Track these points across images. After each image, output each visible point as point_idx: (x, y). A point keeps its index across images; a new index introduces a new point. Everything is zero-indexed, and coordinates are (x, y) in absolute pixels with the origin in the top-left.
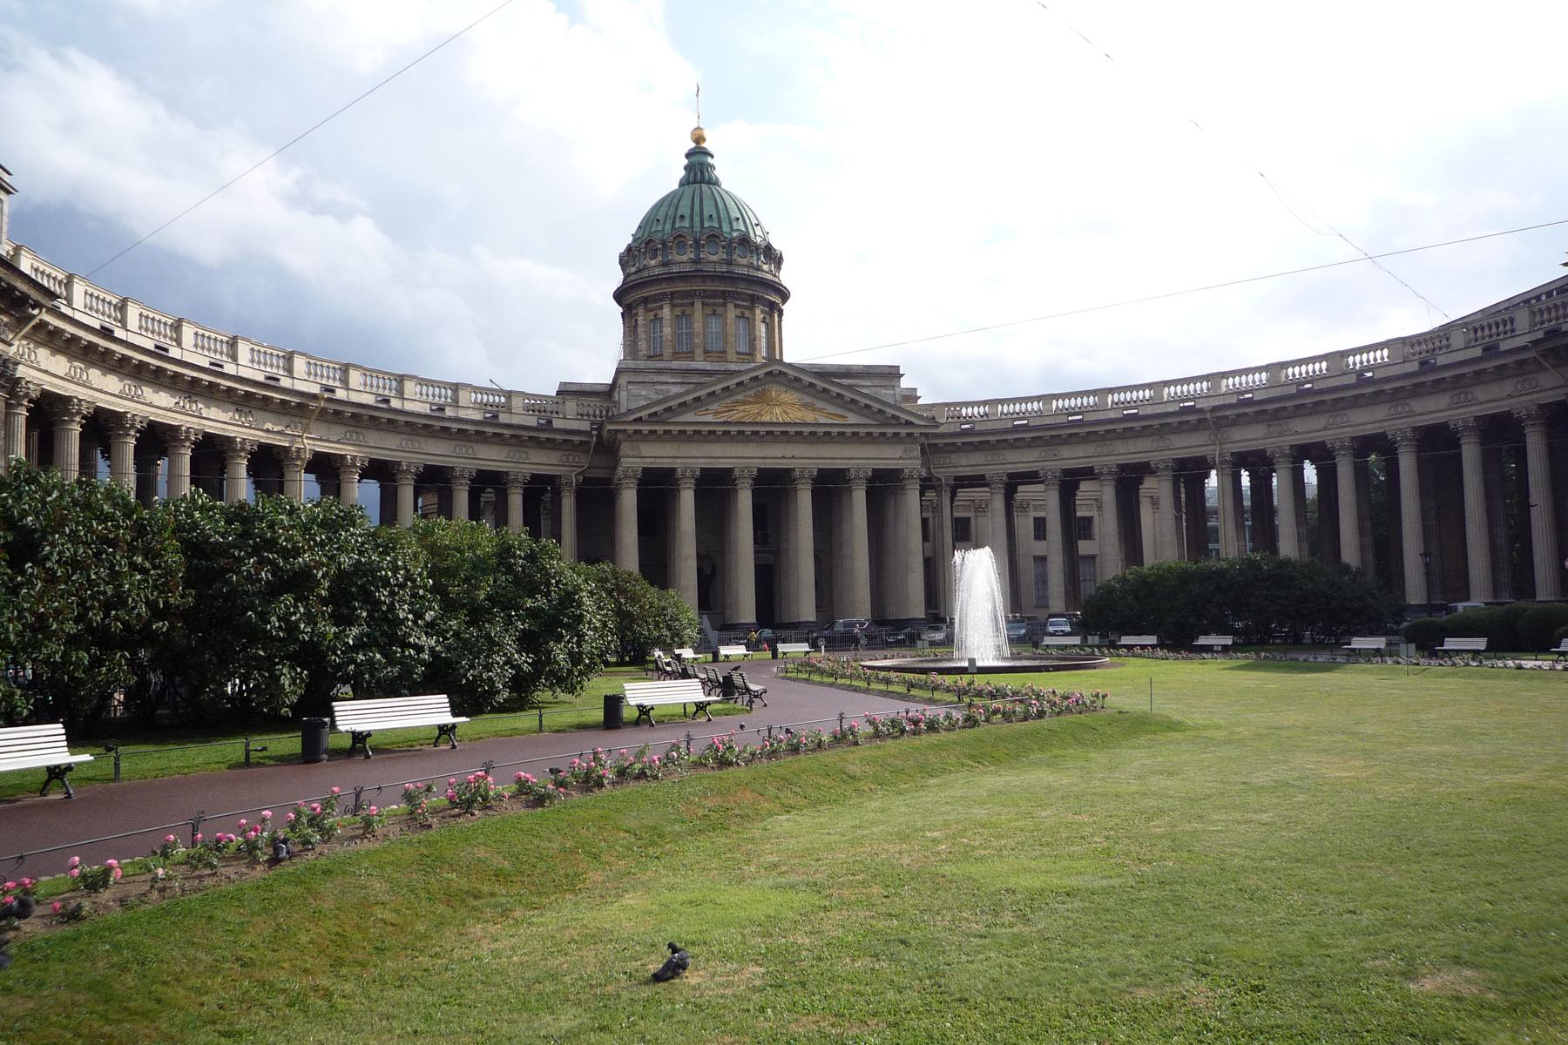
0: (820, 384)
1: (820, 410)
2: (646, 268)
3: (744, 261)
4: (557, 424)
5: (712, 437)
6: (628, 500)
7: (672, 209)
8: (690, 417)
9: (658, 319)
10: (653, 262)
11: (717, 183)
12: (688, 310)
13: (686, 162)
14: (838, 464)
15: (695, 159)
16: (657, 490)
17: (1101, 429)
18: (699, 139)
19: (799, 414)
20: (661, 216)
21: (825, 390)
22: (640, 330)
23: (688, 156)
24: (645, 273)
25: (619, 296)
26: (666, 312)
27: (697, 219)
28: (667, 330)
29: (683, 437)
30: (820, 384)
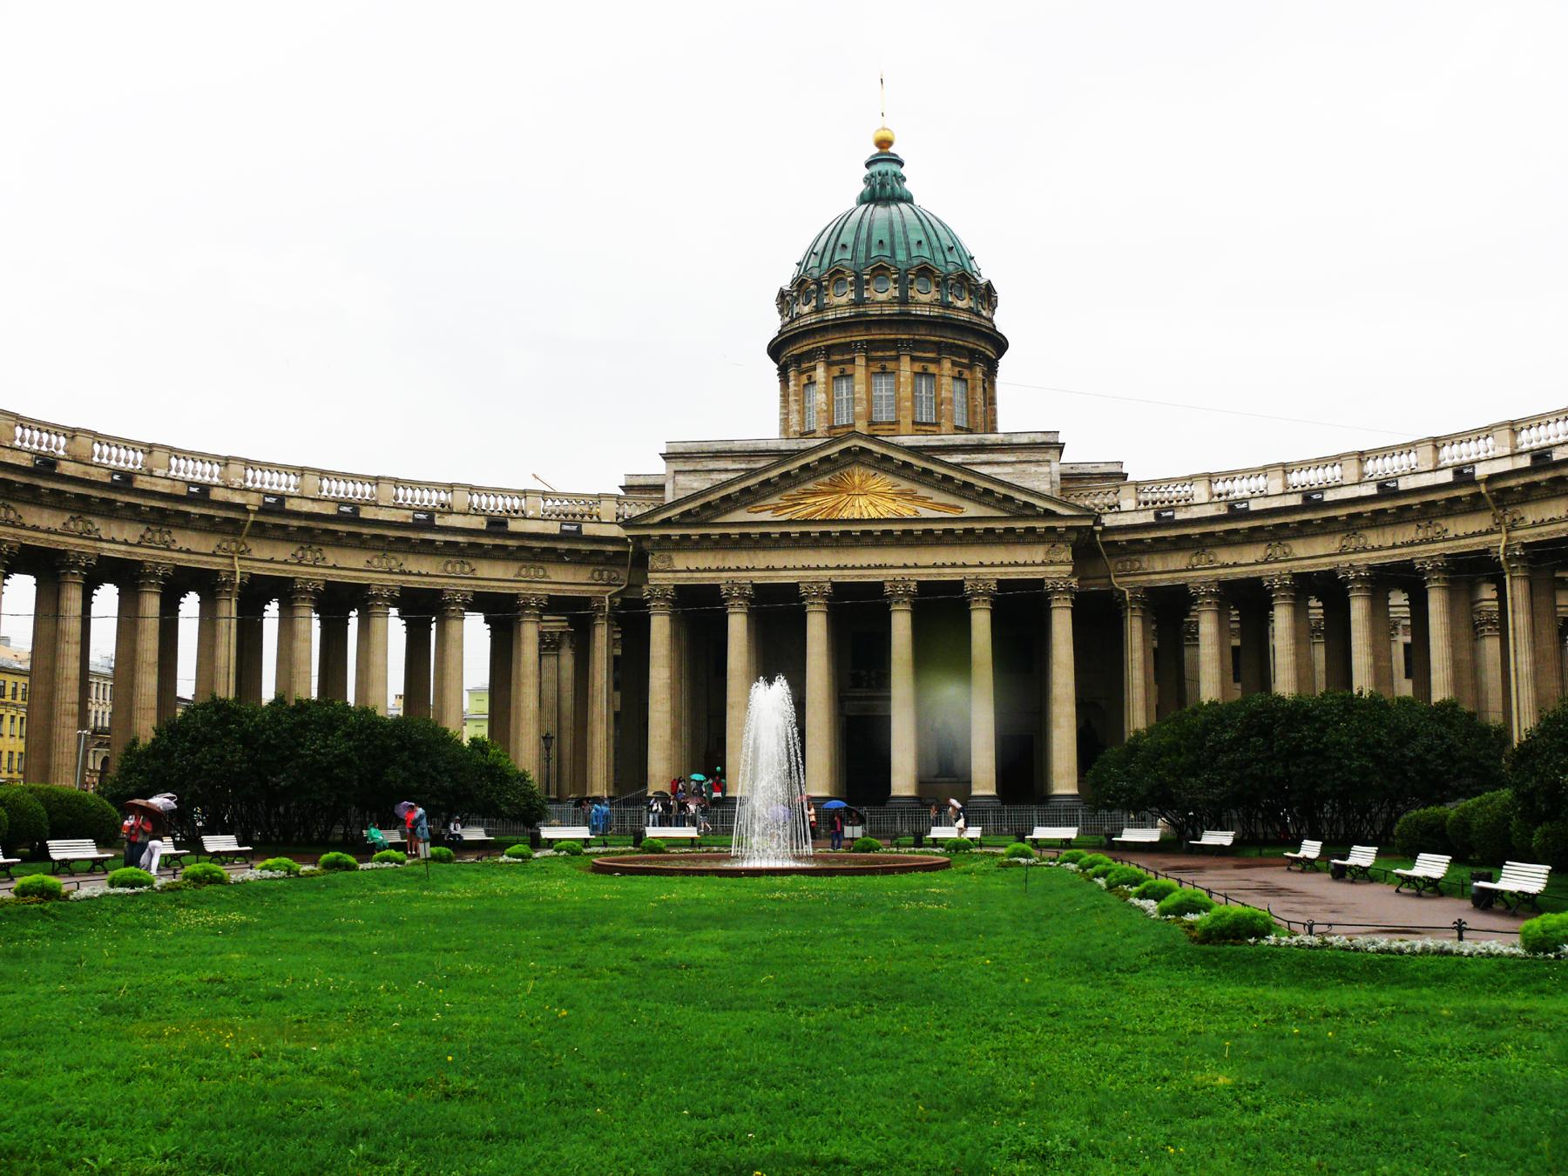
0: (919, 464)
1: (924, 499)
2: (800, 316)
4: (589, 529)
9: (812, 383)
10: (806, 309)
12: (849, 369)
13: (867, 172)
15: (876, 168)
16: (700, 613)
17: (1341, 512)
18: (884, 144)
19: (893, 506)
20: (819, 248)
22: (792, 398)
23: (868, 165)
24: (796, 324)
25: (775, 350)
26: (820, 373)
27: (862, 248)
29: (725, 543)
30: (919, 464)
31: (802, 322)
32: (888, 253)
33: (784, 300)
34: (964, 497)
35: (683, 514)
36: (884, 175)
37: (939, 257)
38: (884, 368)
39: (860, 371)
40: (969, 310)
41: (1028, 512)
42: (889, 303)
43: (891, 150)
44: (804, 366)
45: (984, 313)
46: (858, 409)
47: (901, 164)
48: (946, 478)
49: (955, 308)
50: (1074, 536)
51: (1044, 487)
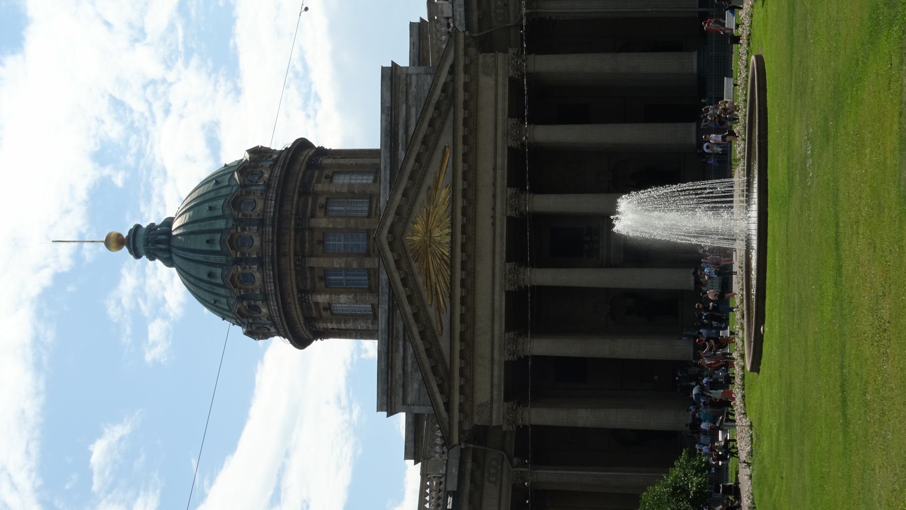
2: (270, 318)
3: (260, 205)
5: (468, 319)
6: (541, 416)
7: (201, 284)
8: (444, 343)
9: (328, 307)
10: (264, 310)
11: (169, 222)
13: (144, 257)
14: (502, 160)
20: (210, 298)
21: (411, 178)
22: (343, 326)
23: (137, 256)
25: (301, 342)
26: (322, 299)
27: (212, 258)
28: (343, 298)
31: (275, 314)
32: (218, 236)
33: (257, 331)
34: (436, 145)
35: (442, 392)
36: (147, 242)
37: (224, 192)
38: (319, 242)
39: (322, 262)
40: (272, 167)
41: (450, 90)
42: (262, 234)
43: (125, 234)
44: (314, 312)
45: (275, 156)
46: (355, 265)
47: (138, 227)
48: (417, 160)
49: (270, 179)
50: (472, 51)
51: (429, 79)
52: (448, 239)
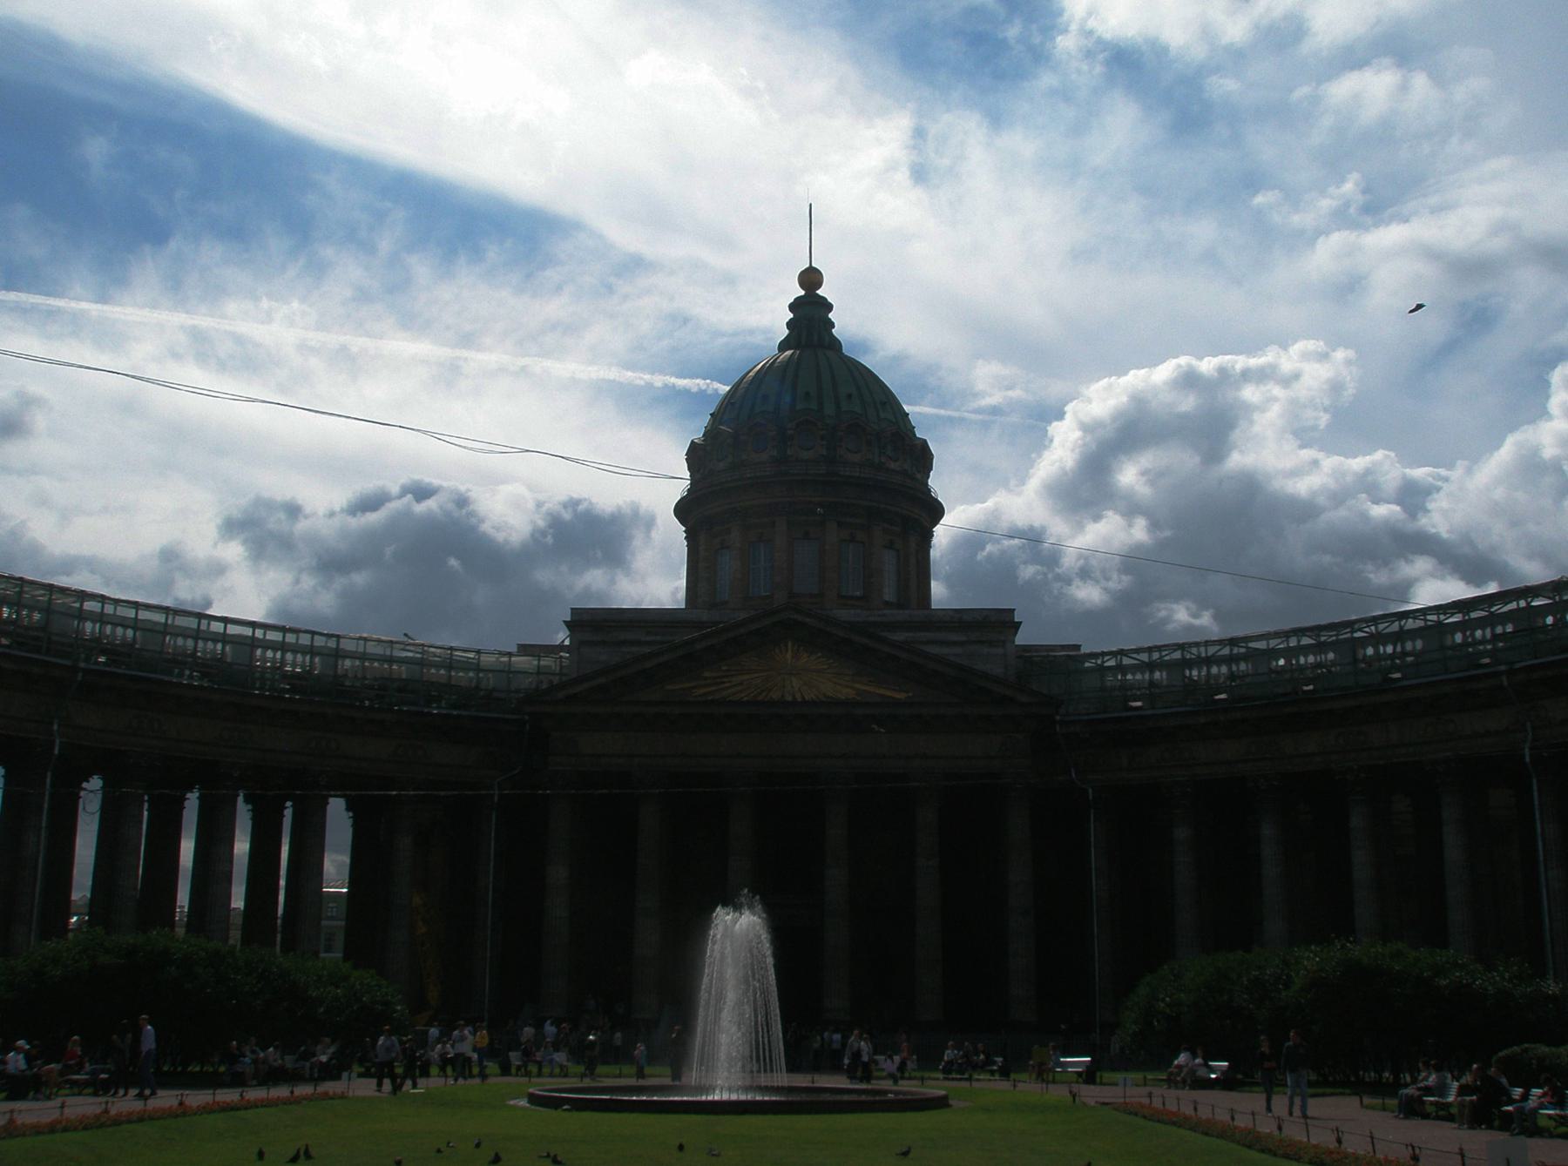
45: (919, 476)
47: (829, 307)
52: (790, 699)
